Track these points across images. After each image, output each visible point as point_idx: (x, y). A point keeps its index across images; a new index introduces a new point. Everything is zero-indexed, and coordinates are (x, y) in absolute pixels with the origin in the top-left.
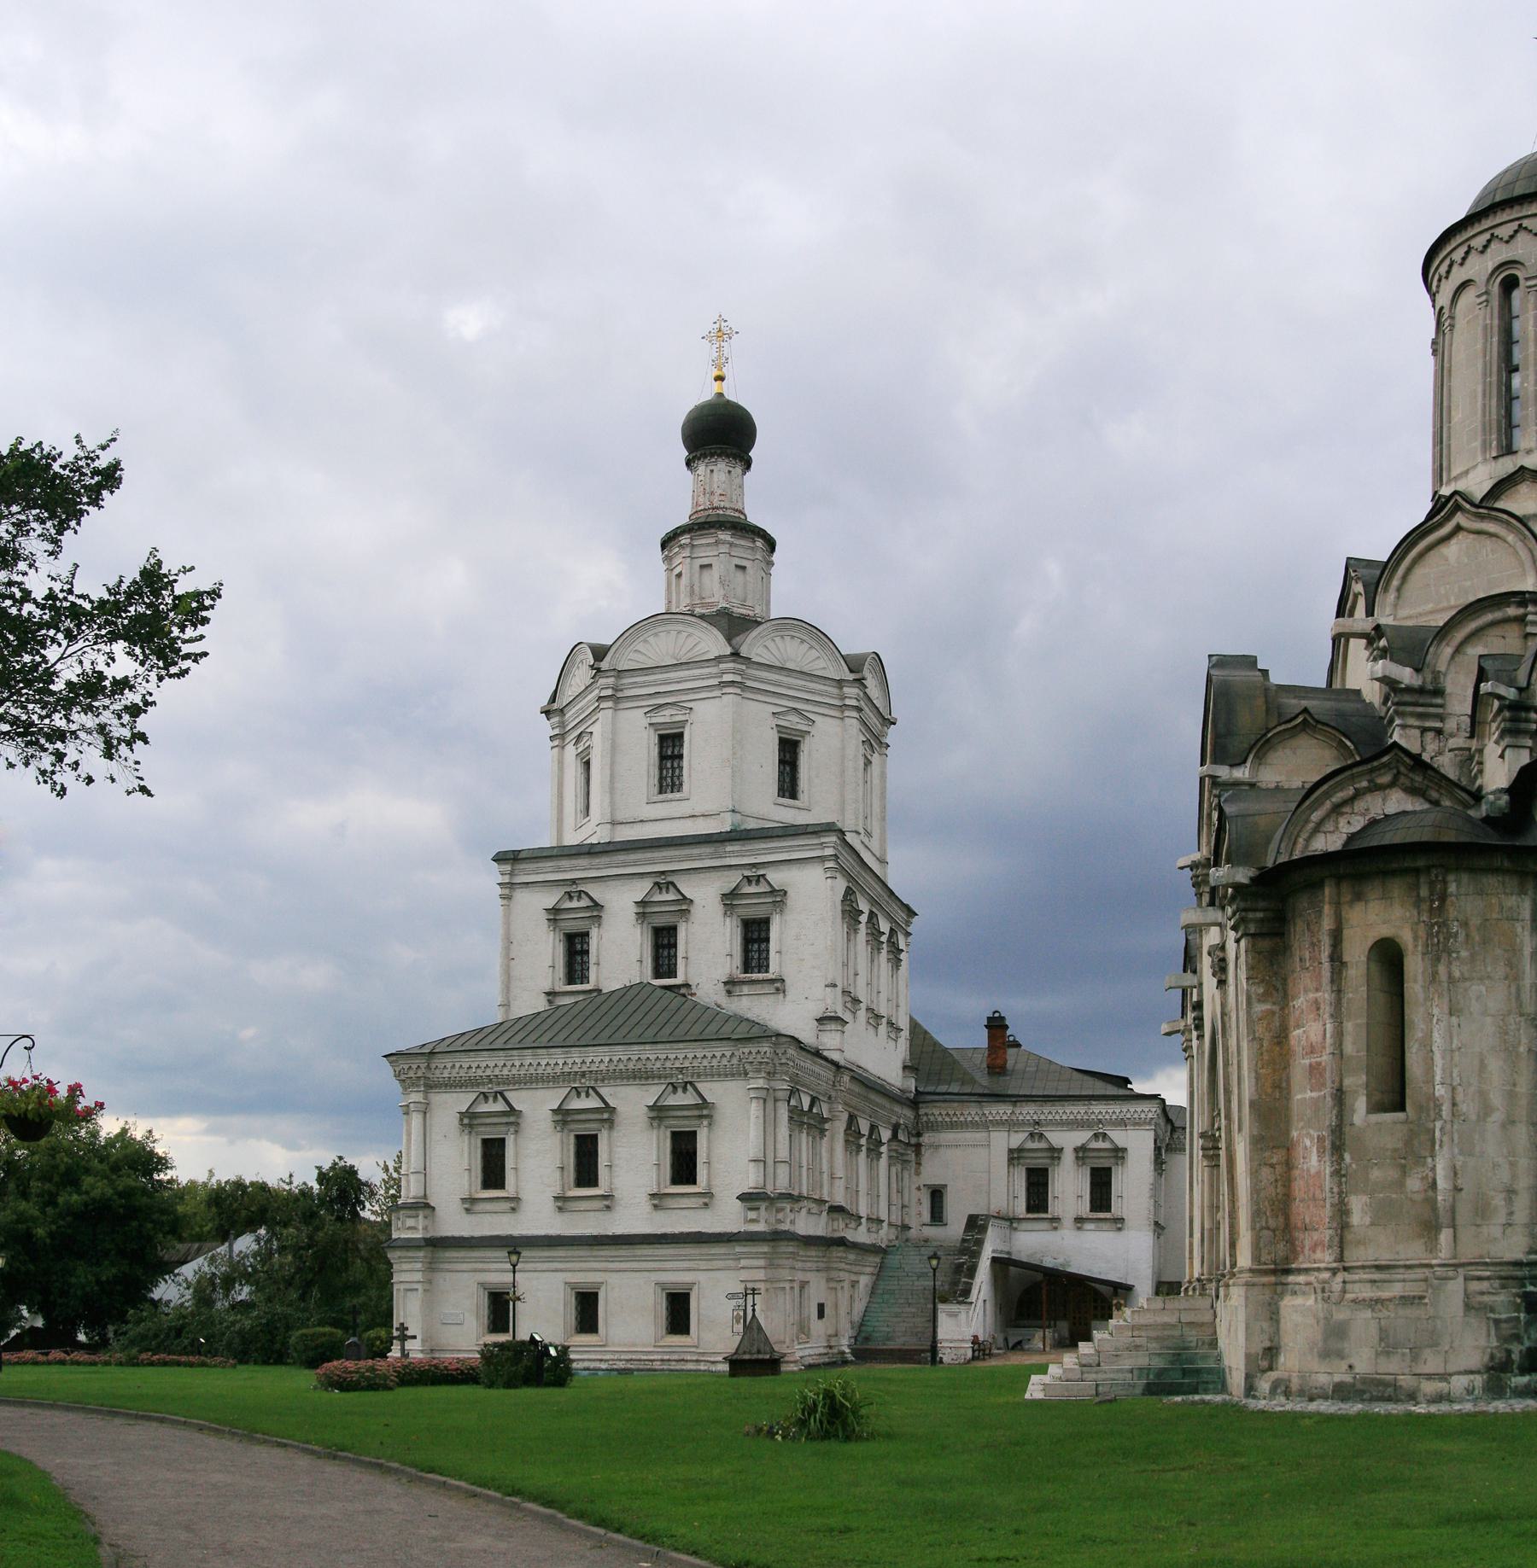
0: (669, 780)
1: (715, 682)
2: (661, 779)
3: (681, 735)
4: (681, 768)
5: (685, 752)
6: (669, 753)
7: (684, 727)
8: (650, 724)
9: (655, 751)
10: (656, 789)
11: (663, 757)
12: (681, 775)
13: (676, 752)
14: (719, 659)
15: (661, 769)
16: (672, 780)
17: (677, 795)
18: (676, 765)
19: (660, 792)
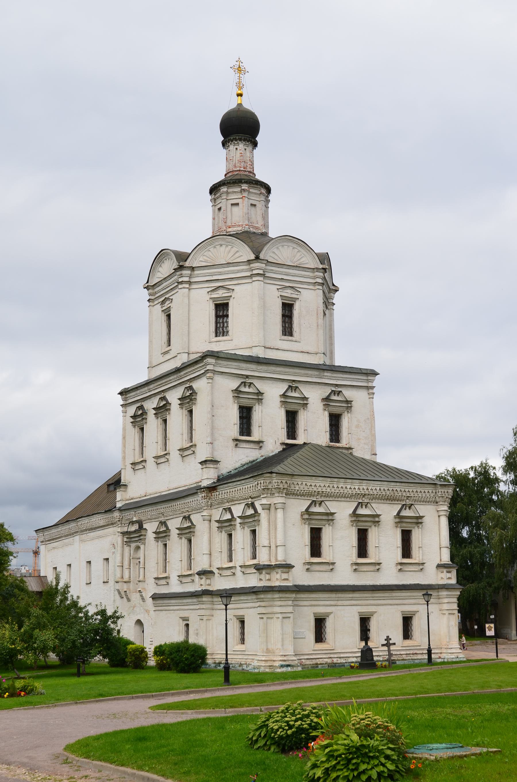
0: (221, 329)
1: (248, 274)
2: (217, 328)
3: (227, 305)
4: (227, 322)
5: (230, 313)
6: (221, 314)
7: (229, 300)
8: (210, 298)
9: (213, 313)
10: (214, 334)
11: (217, 316)
12: (227, 326)
13: (224, 314)
14: (249, 262)
15: (217, 323)
16: (223, 330)
17: (225, 338)
18: (224, 321)
19: (216, 336)
